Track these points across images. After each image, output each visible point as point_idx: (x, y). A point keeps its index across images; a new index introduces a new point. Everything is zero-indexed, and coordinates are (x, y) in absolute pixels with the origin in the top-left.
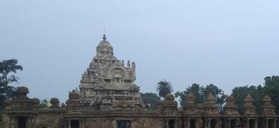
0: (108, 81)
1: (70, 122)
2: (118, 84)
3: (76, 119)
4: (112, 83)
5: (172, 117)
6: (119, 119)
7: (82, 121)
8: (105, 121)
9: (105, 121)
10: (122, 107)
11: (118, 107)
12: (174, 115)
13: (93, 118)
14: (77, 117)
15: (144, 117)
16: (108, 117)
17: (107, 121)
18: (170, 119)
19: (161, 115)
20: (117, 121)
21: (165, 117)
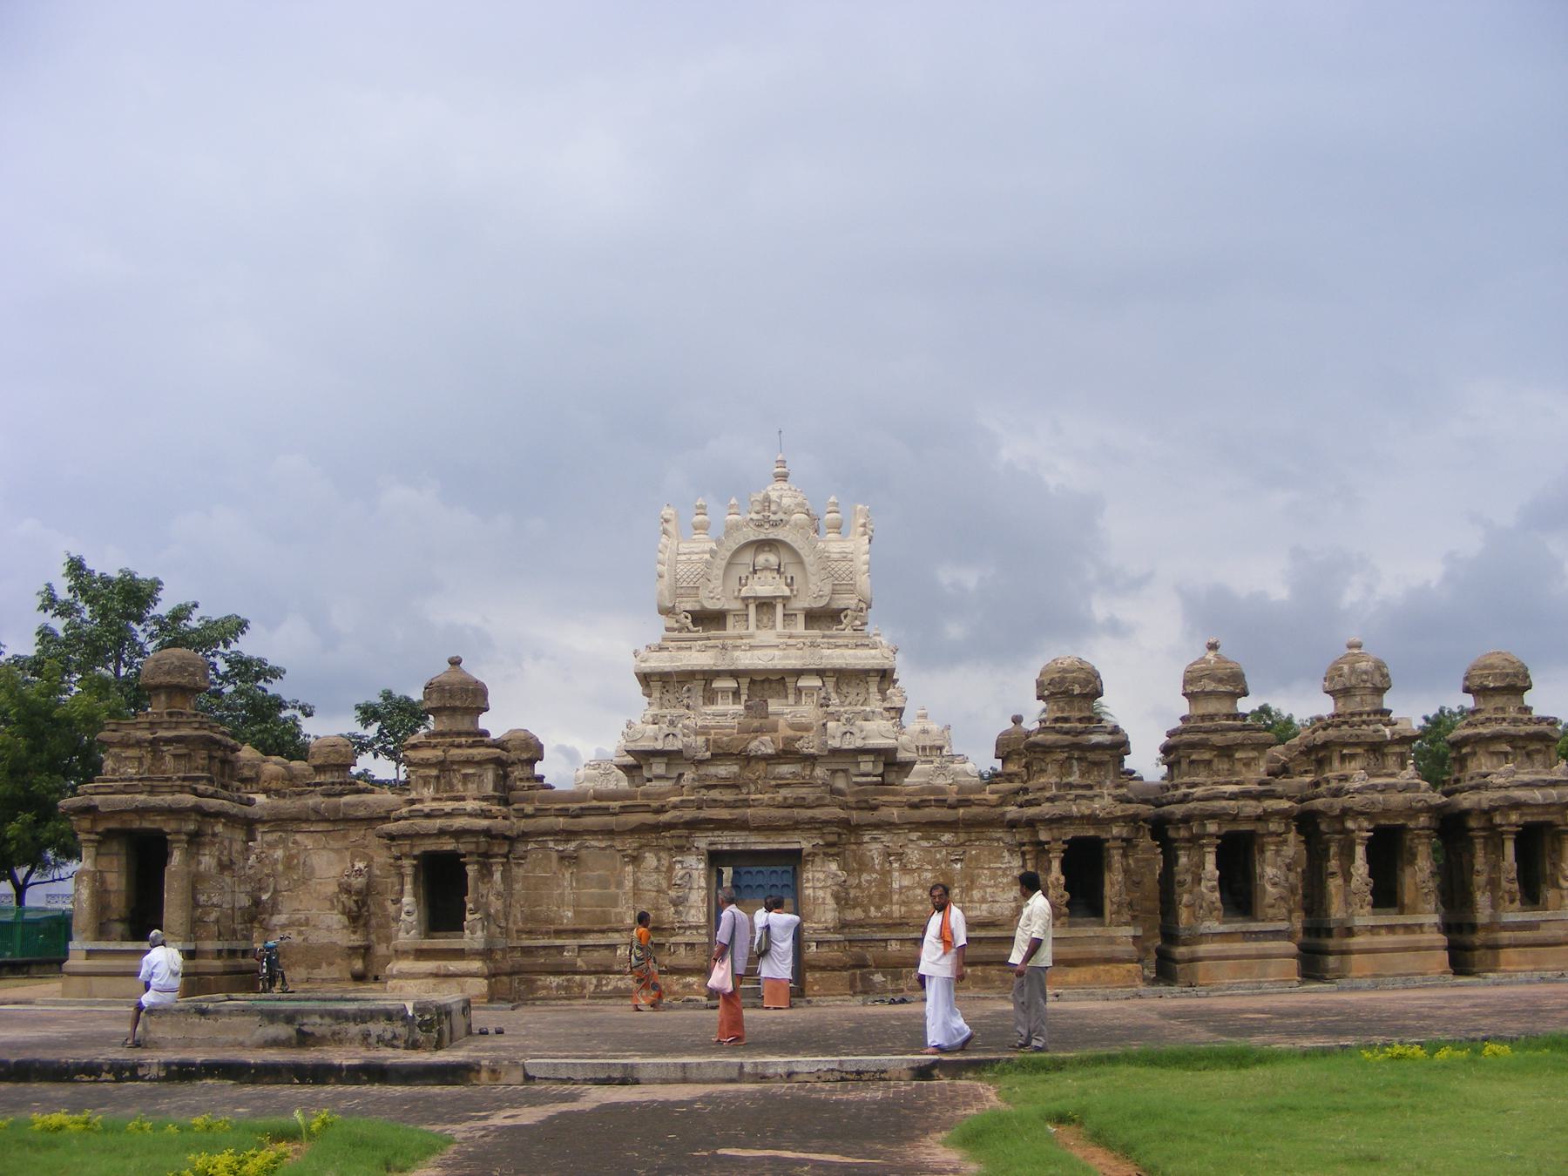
0: (709, 619)
1: (408, 865)
3: (448, 845)
5: (1092, 819)
6: (726, 841)
7: (485, 859)
8: (635, 860)
9: (635, 860)
10: (746, 759)
11: (720, 755)
12: (1103, 804)
13: (569, 835)
14: (458, 834)
15: (887, 826)
16: (657, 828)
17: (650, 860)
18: (1070, 833)
19: (1012, 811)
20: (716, 859)
21: (1031, 823)
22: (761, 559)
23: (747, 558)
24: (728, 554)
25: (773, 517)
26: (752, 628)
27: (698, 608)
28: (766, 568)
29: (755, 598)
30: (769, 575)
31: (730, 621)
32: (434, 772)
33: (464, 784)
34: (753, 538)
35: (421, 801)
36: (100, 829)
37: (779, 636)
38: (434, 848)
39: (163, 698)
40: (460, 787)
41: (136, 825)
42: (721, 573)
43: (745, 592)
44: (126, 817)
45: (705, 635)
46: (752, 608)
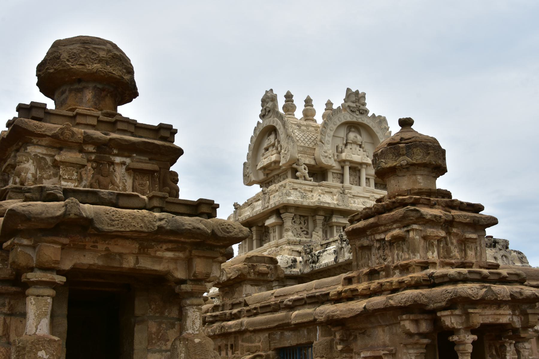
2: (356, 190)
3: (505, 316)
4: (331, 181)
22: (352, 135)
23: (342, 133)
24: (335, 127)
25: (362, 107)
26: (347, 183)
27: (313, 163)
28: (355, 143)
29: (351, 162)
30: (354, 146)
31: (330, 176)
32: (443, 234)
33: (464, 251)
34: (349, 119)
35: (434, 264)
36: (67, 265)
37: (368, 191)
38: (490, 320)
39: (89, 95)
40: (456, 252)
41: (129, 263)
42: (330, 139)
43: (344, 156)
44: (116, 248)
45: (317, 184)
46: (347, 169)
